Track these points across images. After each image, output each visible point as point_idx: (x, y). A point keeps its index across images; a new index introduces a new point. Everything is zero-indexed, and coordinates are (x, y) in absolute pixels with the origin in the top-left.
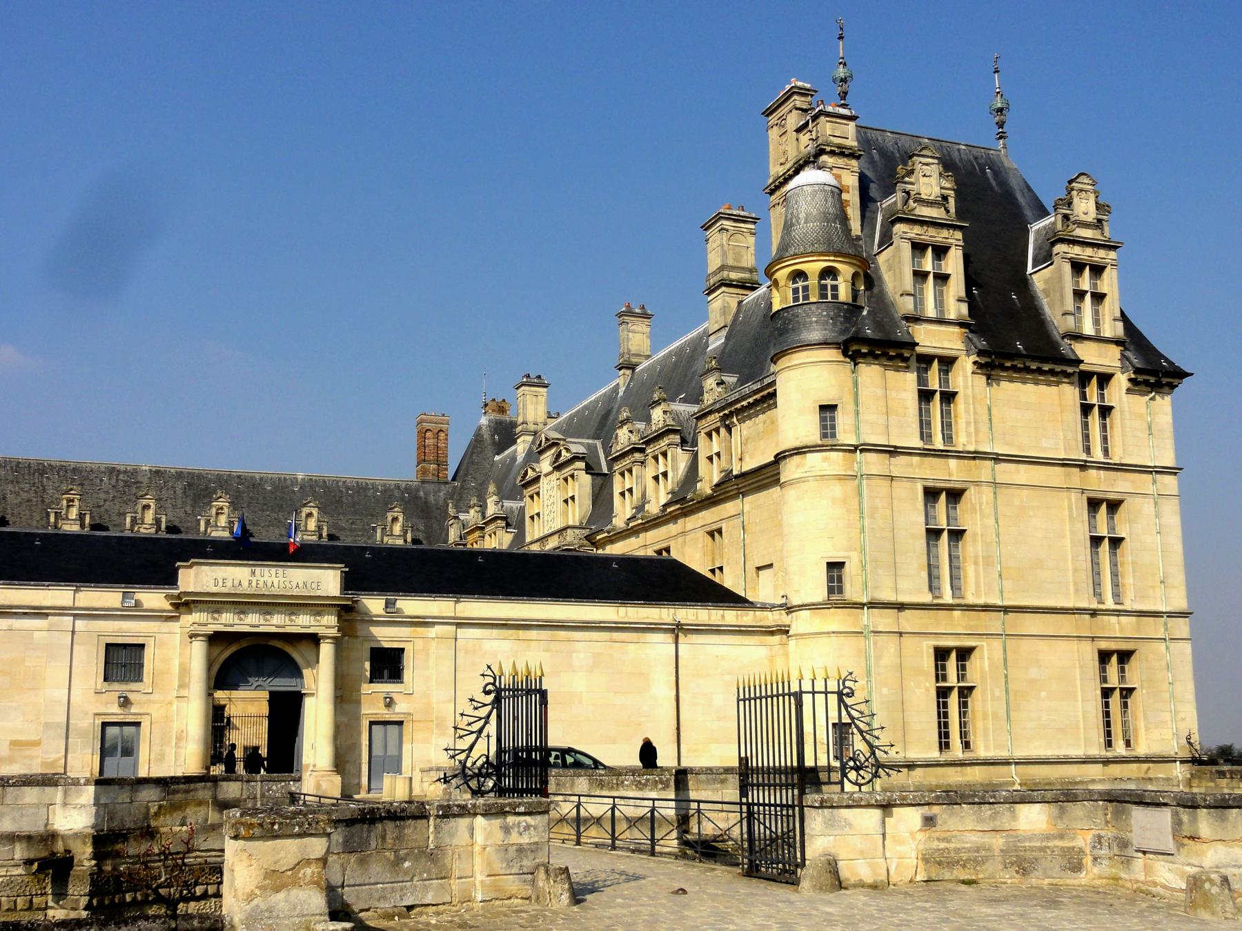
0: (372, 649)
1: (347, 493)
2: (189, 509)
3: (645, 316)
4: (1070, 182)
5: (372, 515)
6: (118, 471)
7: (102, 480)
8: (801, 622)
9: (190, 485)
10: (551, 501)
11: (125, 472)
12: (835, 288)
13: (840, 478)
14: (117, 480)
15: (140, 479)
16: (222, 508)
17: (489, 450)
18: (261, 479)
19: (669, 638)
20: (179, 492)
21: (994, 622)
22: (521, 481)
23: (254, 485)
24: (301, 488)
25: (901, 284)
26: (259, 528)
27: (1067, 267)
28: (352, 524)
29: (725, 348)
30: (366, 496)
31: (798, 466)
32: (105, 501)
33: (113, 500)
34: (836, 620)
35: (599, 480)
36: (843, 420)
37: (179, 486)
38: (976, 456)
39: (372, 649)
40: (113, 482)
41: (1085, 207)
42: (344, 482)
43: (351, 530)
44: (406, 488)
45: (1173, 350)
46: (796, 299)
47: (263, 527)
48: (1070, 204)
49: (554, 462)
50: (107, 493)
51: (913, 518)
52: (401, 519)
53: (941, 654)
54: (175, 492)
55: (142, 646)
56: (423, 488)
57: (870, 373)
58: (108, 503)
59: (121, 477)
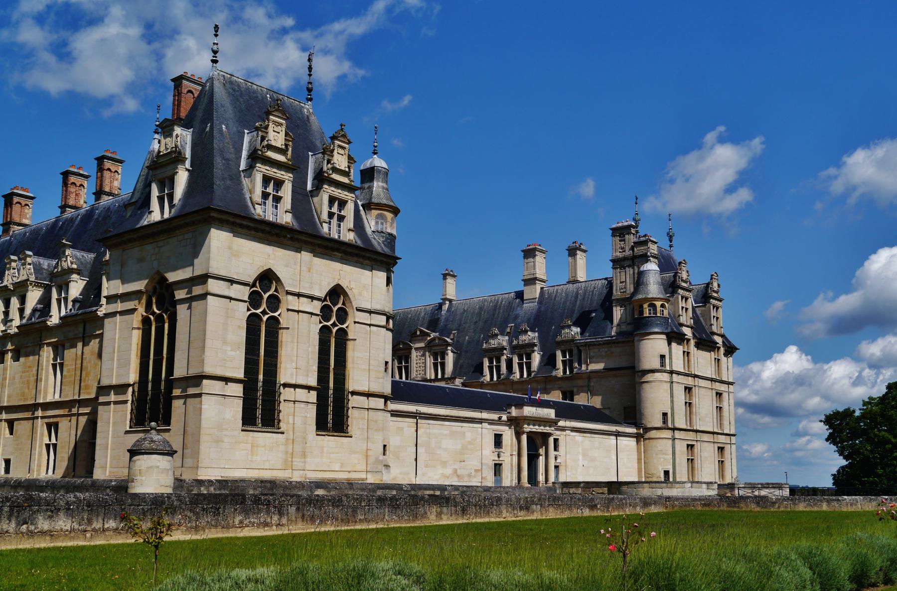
0: (554, 439)
3: (454, 276)
4: (712, 275)
8: (653, 434)
12: (663, 311)
13: (666, 382)
19: (614, 437)
21: (700, 436)
25: (679, 312)
27: (712, 307)
29: (540, 308)
31: (651, 376)
34: (667, 434)
35: (455, 355)
36: (667, 361)
38: (695, 376)
39: (554, 439)
41: (715, 284)
45: (735, 342)
46: (650, 314)
48: (712, 283)
51: (680, 396)
53: (688, 445)
55: (502, 435)
57: (674, 345)
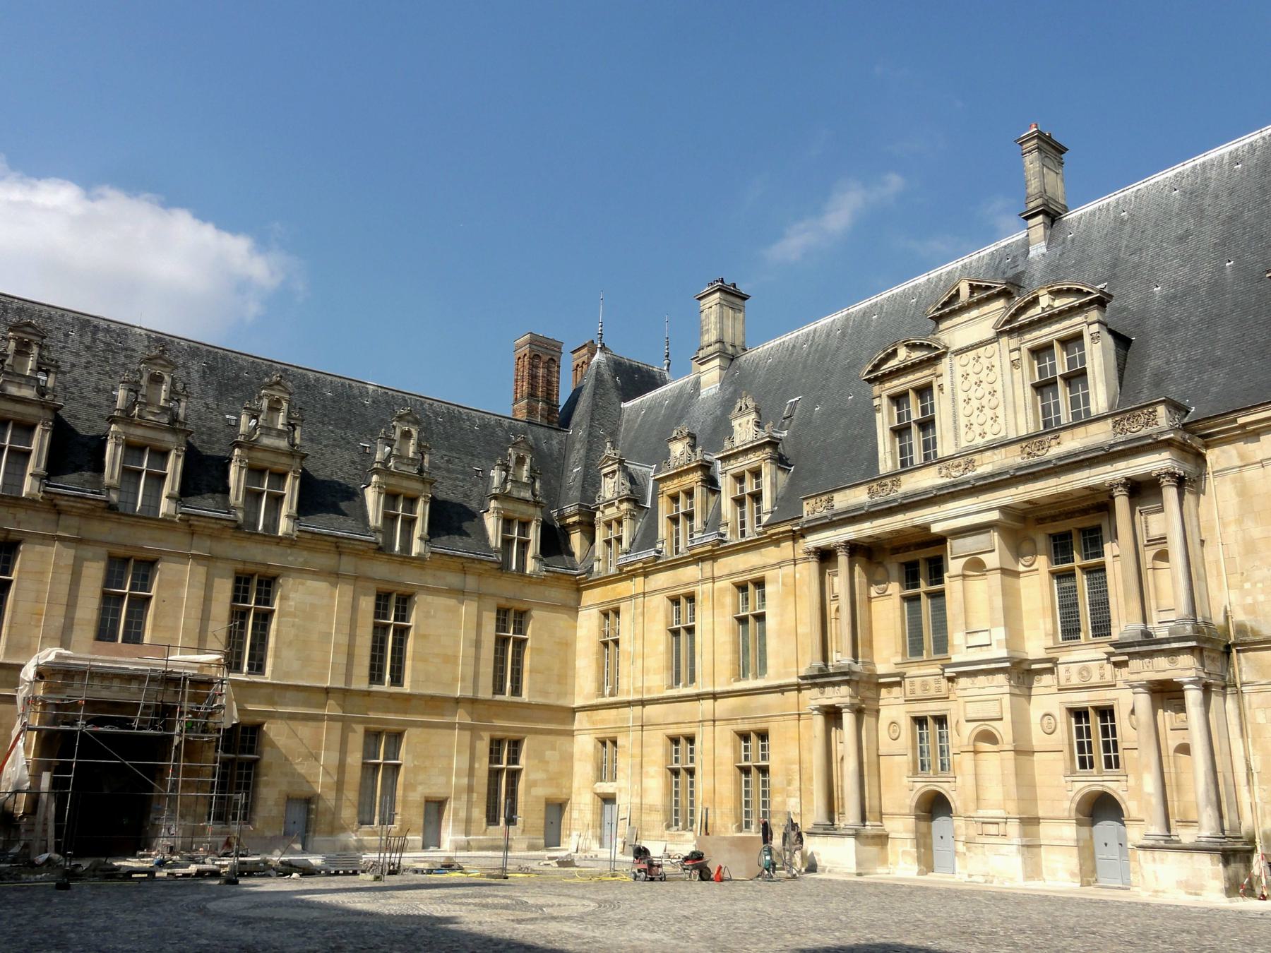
1: (436, 420)
2: (210, 401)
5: (473, 456)
6: (95, 327)
7: (67, 335)
9: (212, 369)
10: (986, 388)
11: (107, 330)
14: (94, 340)
15: (131, 344)
16: (278, 401)
17: (613, 396)
18: (317, 380)
20: (195, 376)
22: (870, 372)
23: (307, 386)
24: (373, 402)
26: (320, 446)
28: (449, 461)
30: (461, 429)
32: (73, 365)
33: (86, 367)
37: (196, 366)
40: (87, 340)
42: (431, 405)
43: (448, 471)
44: (510, 427)
47: (325, 446)
49: (1008, 322)
50: (78, 355)
52: (528, 461)
54: (188, 373)
56: (531, 431)
58: (77, 371)
59: (100, 335)
